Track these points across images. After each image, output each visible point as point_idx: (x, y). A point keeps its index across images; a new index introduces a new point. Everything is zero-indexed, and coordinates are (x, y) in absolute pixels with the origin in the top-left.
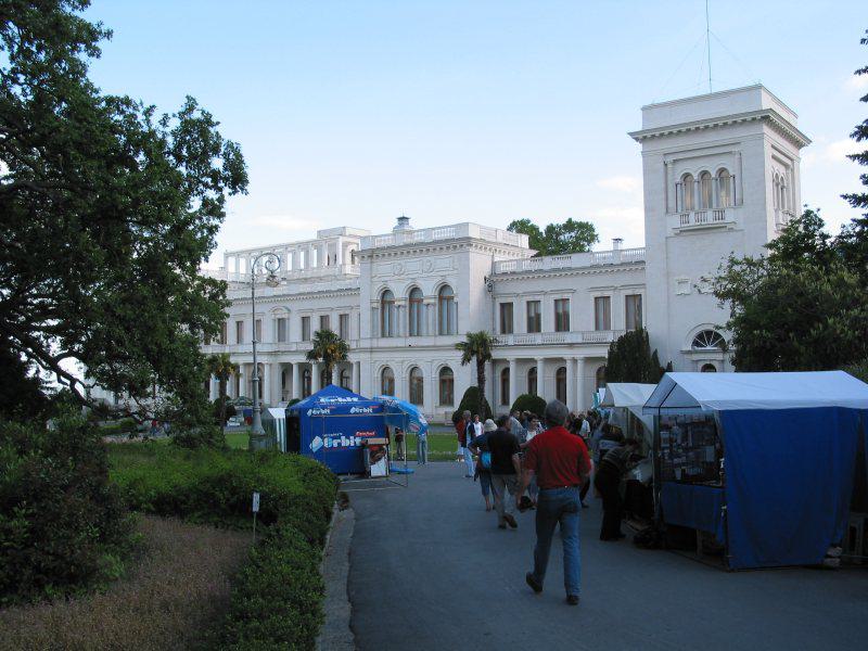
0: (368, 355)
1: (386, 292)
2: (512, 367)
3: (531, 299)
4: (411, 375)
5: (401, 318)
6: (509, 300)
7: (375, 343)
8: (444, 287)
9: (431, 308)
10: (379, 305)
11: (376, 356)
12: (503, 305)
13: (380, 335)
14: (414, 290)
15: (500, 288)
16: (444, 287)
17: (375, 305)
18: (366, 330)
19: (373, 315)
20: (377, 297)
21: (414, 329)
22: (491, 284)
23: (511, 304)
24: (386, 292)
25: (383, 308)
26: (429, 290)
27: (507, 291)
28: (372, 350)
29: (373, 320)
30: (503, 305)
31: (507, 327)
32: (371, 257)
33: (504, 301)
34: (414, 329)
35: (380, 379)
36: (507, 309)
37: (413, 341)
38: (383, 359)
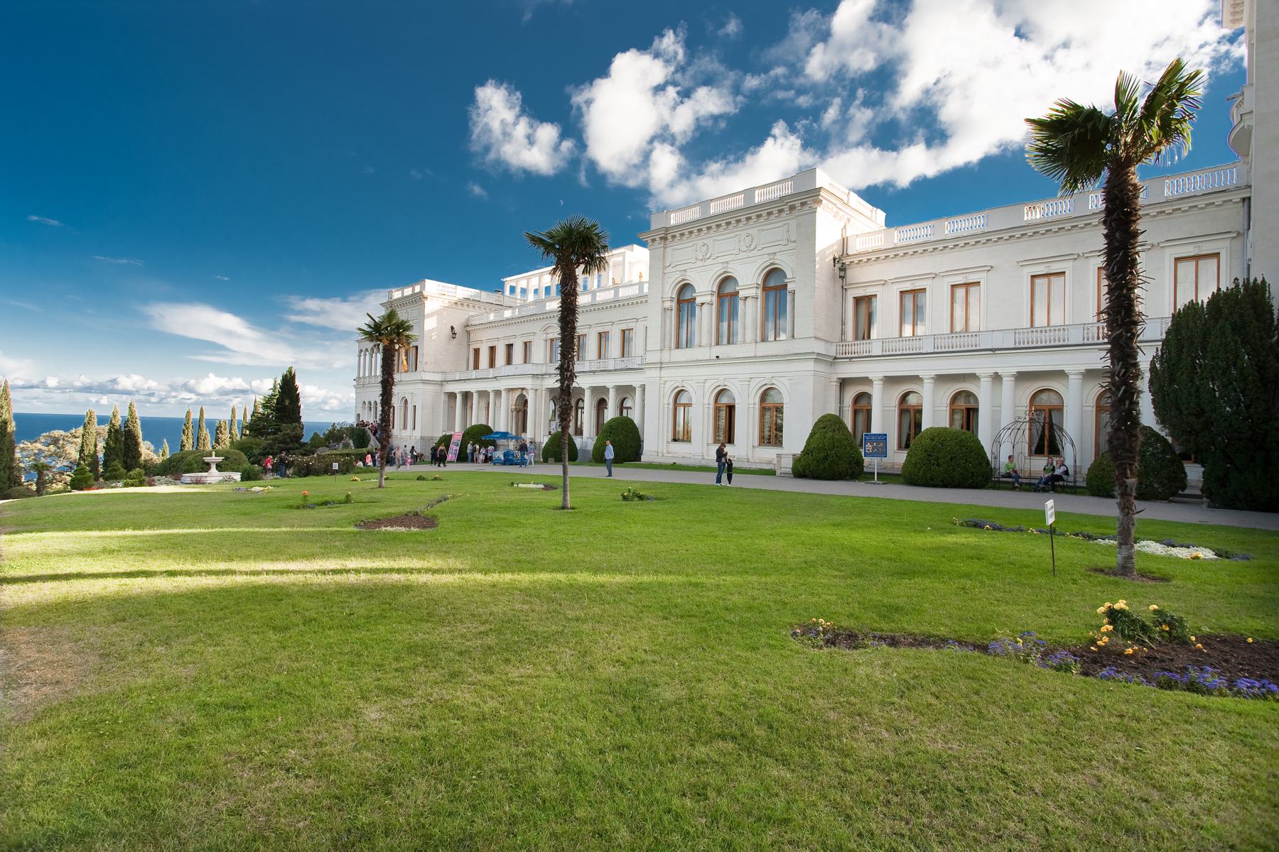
0: (656, 373)
1: (685, 287)
2: (876, 391)
3: (908, 286)
4: (716, 401)
5: (705, 318)
6: (869, 292)
7: (666, 356)
8: (773, 273)
9: (749, 301)
10: (674, 305)
11: (665, 373)
12: (858, 300)
13: (673, 346)
14: (726, 280)
15: (855, 275)
16: (773, 273)
17: (668, 305)
18: (654, 341)
19: (664, 321)
20: (671, 292)
21: (726, 336)
22: (841, 266)
23: (869, 299)
24: (685, 287)
25: (679, 310)
26: (748, 279)
27: (863, 278)
28: (661, 365)
29: (663, 327)
30: (858, 300)
31: (864, 332)
32: (664, 239)
33: (861, 293)
34: (726, 336)
35: (671, 406)
36: (864, 302)
37: (724, 351)
38: (674, 378)
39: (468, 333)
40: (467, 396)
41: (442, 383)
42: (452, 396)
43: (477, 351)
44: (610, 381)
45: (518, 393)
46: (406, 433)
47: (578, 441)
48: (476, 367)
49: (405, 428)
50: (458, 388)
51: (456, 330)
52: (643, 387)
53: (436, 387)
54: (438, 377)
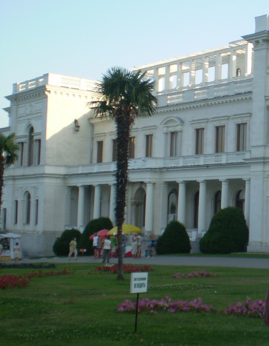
39: (92, 125)
40: (89, 190)
41: (65, 177)
42: (74, 189)
43: (100, 144)
44: (222, 175)
45: (137, 187)
46: (31, 227)
47: (193, 236)
48: (100, 160)
49: (28, 221)
50: (80, 182)
51: (80, 124)
52: (249, 180)
53: (59, 181)
54: (62, 171)
